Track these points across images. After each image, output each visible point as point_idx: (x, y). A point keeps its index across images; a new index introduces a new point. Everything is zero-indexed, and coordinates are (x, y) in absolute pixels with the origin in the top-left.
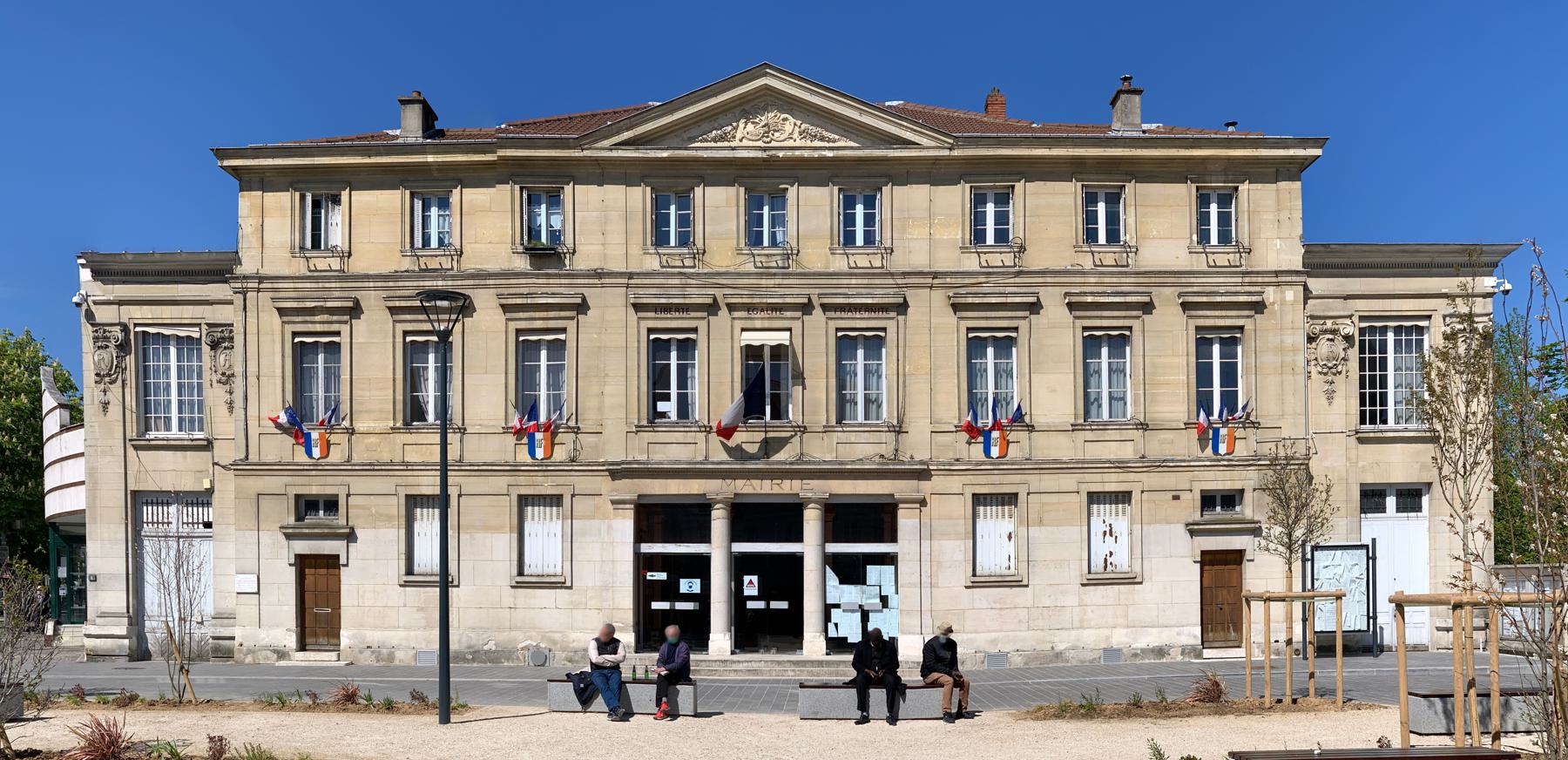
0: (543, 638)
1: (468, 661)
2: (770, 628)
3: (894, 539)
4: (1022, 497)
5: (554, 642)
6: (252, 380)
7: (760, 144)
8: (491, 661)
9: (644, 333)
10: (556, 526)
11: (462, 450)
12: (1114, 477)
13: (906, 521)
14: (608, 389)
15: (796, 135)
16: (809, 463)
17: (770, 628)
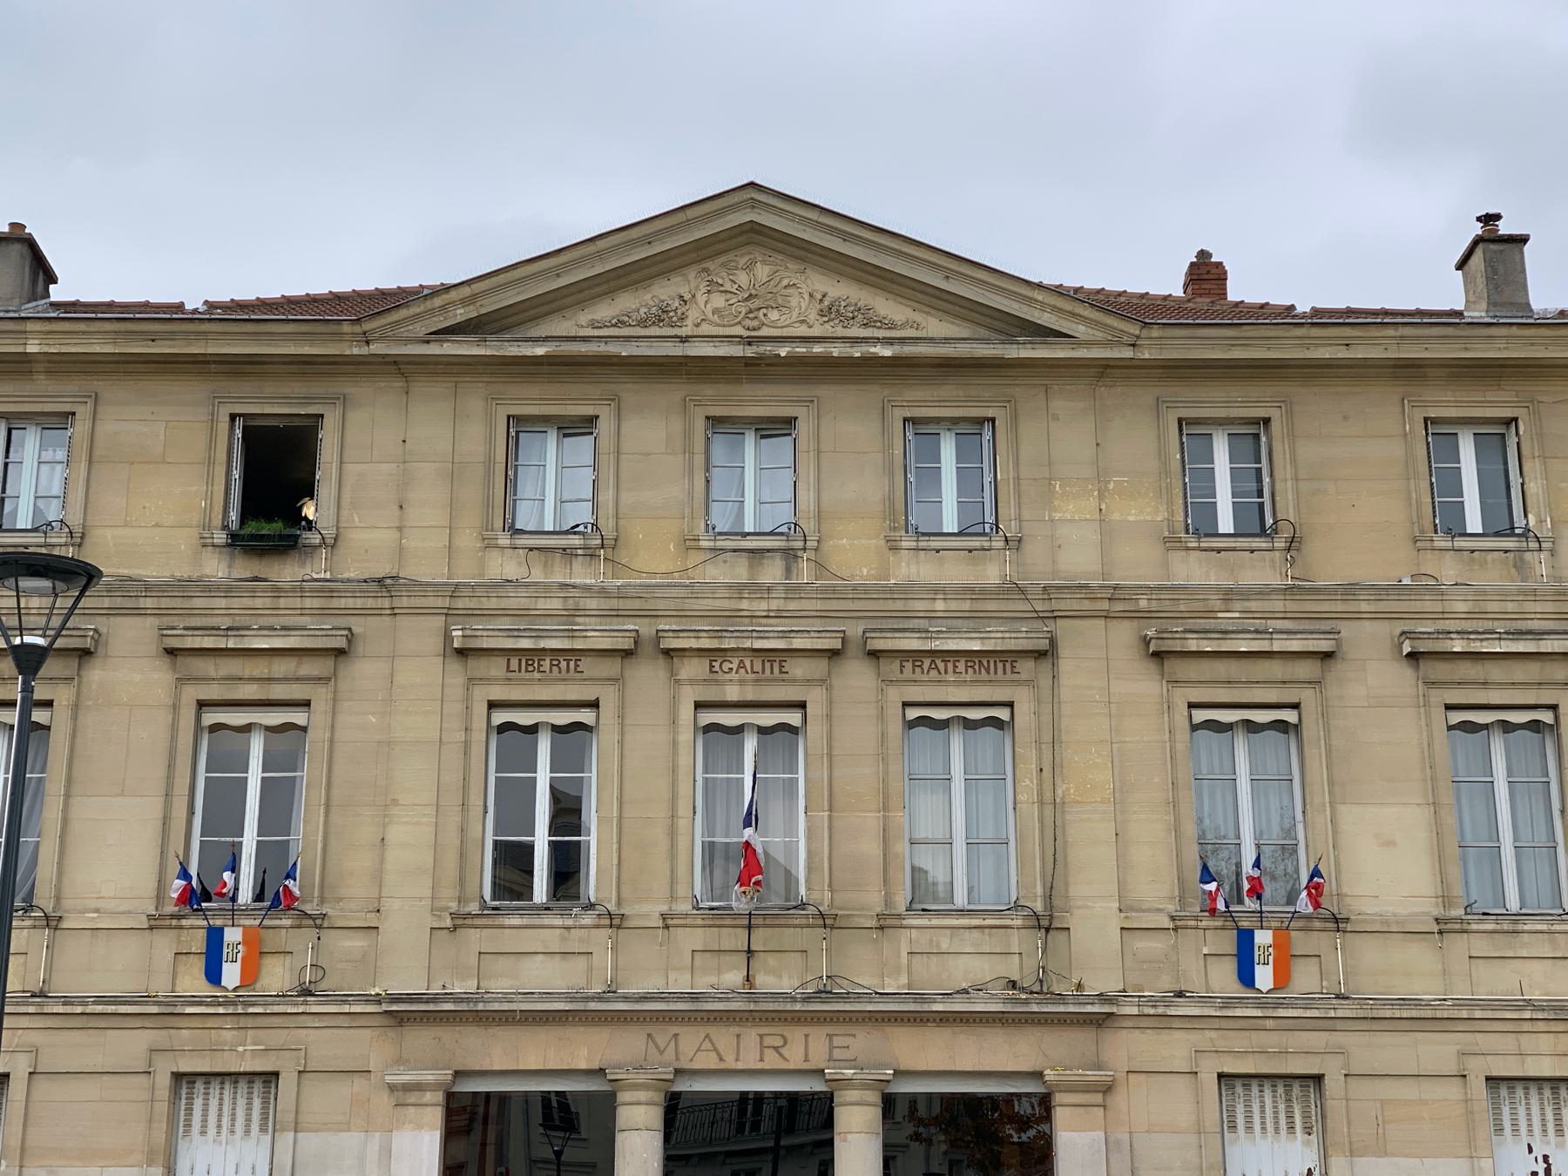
4: (1333, 1084)
7: (739, 331)
11: (49, 969)
12: (1545, 1043)
14: (395, 834)
15: (813, 316)
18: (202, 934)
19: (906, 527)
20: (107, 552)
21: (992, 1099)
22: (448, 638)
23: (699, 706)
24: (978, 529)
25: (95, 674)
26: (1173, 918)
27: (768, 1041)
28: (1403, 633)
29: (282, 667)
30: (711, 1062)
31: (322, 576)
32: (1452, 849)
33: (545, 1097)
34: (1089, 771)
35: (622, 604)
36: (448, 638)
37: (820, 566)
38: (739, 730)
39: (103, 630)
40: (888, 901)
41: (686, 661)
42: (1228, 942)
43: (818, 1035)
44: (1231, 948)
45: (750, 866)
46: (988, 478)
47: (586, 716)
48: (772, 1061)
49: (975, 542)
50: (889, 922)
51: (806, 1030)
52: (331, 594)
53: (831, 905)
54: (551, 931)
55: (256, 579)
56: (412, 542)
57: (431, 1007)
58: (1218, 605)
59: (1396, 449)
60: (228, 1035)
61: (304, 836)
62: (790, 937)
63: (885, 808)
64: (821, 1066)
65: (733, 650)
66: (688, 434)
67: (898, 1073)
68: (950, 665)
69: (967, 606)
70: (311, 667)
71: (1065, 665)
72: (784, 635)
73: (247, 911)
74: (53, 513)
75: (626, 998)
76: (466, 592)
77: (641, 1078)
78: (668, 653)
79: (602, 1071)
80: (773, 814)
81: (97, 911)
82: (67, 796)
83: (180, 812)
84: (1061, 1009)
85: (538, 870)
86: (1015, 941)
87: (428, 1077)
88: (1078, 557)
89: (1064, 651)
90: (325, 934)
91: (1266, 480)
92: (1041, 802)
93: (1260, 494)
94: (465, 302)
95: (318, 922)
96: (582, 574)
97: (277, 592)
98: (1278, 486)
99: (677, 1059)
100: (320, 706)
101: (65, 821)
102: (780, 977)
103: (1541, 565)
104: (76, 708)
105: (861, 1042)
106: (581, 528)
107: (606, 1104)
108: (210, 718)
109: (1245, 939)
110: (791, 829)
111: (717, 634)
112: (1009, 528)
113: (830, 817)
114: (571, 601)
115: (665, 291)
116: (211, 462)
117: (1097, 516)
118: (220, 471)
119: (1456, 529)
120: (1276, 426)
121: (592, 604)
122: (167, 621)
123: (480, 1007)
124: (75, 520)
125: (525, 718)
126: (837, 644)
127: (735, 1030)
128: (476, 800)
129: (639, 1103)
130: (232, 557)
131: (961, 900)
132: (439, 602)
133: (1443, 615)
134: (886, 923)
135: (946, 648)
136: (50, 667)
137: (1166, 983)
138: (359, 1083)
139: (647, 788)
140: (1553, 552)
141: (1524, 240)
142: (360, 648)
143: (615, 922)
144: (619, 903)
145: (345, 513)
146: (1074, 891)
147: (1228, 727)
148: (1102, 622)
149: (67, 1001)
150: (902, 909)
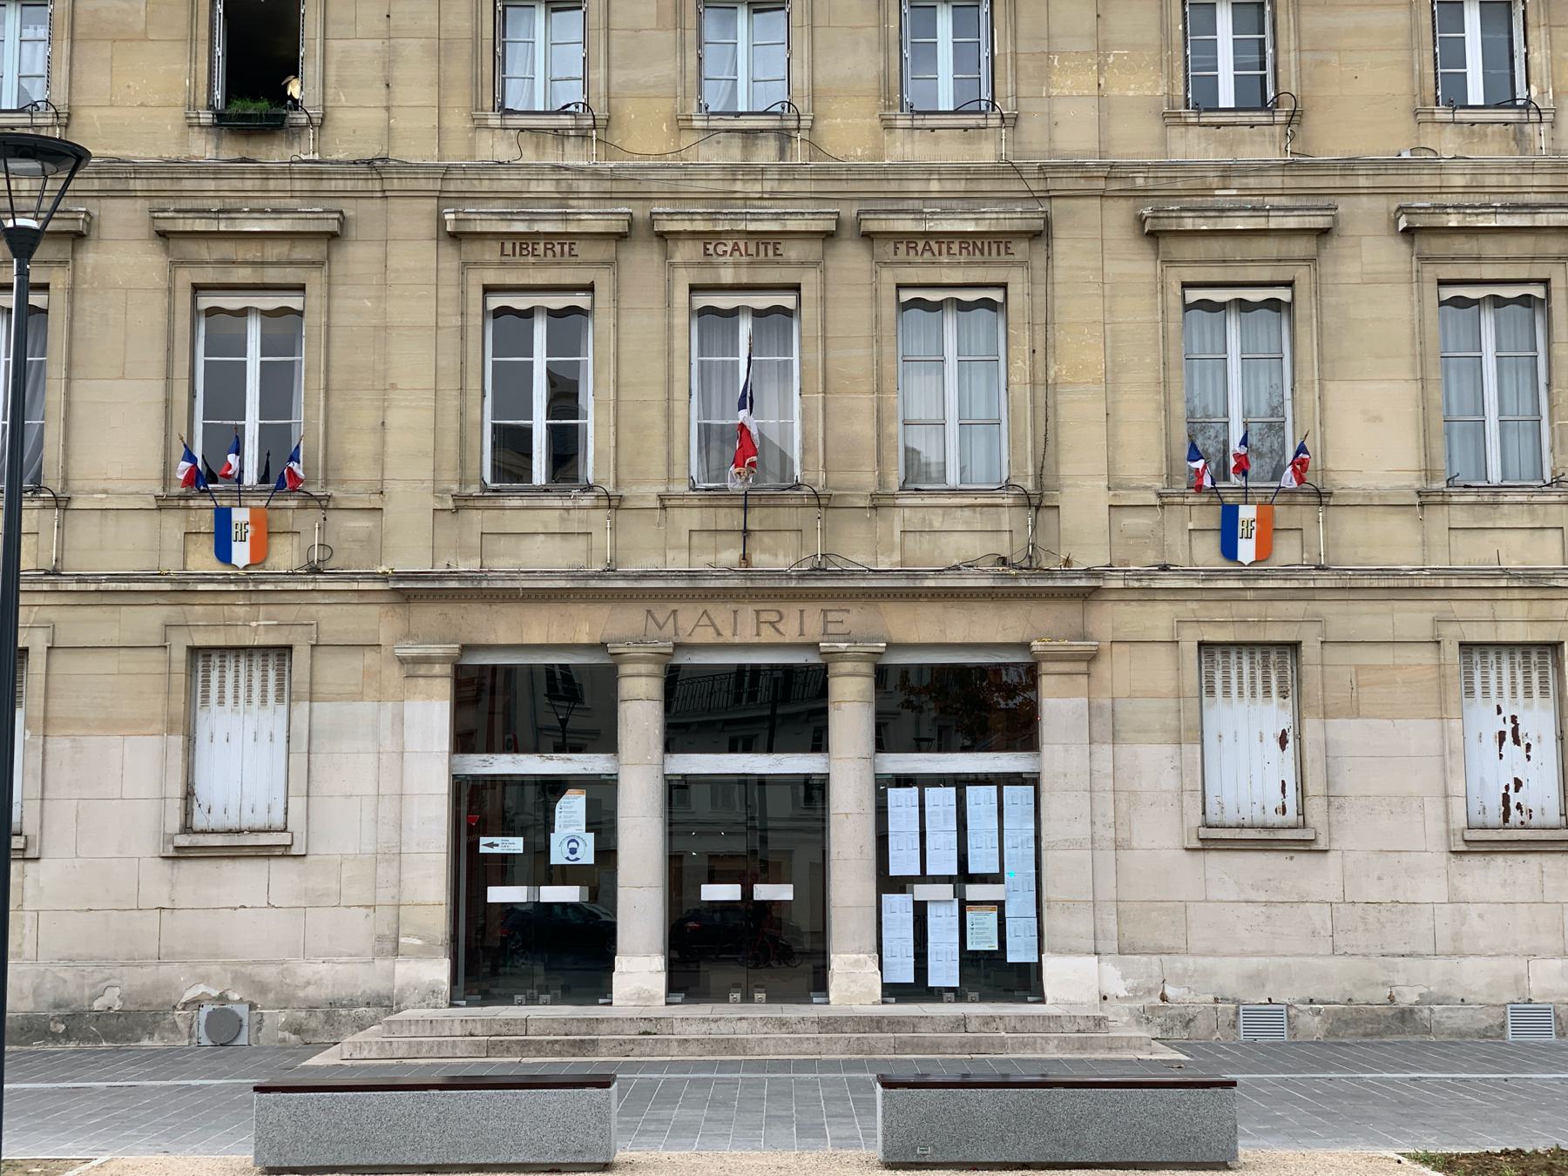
0: (237, 978)
1: (55, 1037)
2: (745, 944)
4: (1309, 651)
5: (262, 988)
8: (109, 1037)
9: (476, 294)
11: (61, 547)
12: (1519, 610)
13: (1059, 706)
14: (395, 418)
16: (840, 574)
17: (745, 944)
18: (210, 514)
19: (900, 105)
20: (97, 132)
21: (982, 670)
22: (441, 221)
23: (694, 289)
24: (974, 106)
25: (90, 257)
26: (1160, 495)
27: (764, 617)
28: (1400, 208)
29: (274, 251)
31: (311, 157)
32: (1437, 423)
33: (550, 669)
34: (1080, 352)
35: (615, 186)
36: (441, 221)
38: (734, 312)
39: (95, 212)
40: (882, 482)
41: (680, 244)
42: (1212, 518)
43: (813, 612)
45: (745, 447)
46: (985, 53)
47: (582, 300)
48: (768, 635)
49: (970, 121)
50: (882, 502)
51: (801, 606)
52: (319, 175)
53: (826, 486)
54: (550, 513)
56: (400, 122)
57: (437, 585)
58: (1216, 182)
59: (1400, 18)
60: (241, 611)
61: (306, 418)
62: (785, 517)
64: (816, 640)
65: (727, 232)
67: (890, 646)
68: (944, 247)
69: (961, 186)
70: (303, 251)
71: (1060, 246)
73: (252, 493)
74: (37, 93)
75: (625, 577)
76: (457, 174)
78: (663, 236)
80: (768, 397)
81: (105, 492)
82: (69, 379)
83: (181, 395)
84: (1050, 583)
85: (535, 452)
86: (1006, 519)
87: (437, 650)
89: (1059, 232)
90: (333, 517)
91: (1269, 51)
92: (1033, 384)
93: (1263, 67)
95: (324, 503)
96: (574, 156)
97: (266, 174)
98: (1282, 58)
99: (676, 634)
101: (68, 404)
102: (776, 555)
103: (1540, 138)
104: (72, 291)
105: (854, 618)
106: (572, 108)
107: (607, 678)
108: (206, 302)
109: (1230, 514)
110: (785, 411)
111: (711, 217)
112: (1006, 105)
113: (824, 398)
114: (563, 184)
116: (193, 39)
117: (1096, 92)
118: (203, 49)
119: (1457, 100)
121: (585, 186)
122: (157, 203)
123: (484, 584)
124: (60, 99)
125: (520, 302)
126: (831, 226)
127: (732, 606)
128: (473, 384)
129: (640, 676)
130: (219, 138)
131: (953, 479)
132: (431, 185)
133: (1441, 190)
134: (879, 503)
135: (939, 229)
136: (44, 251)
137: (1152, 557)
138: (370, 657)
139: (643, 374)
140: (1553, 124)
142: (352, 232)
143: (614, 503)
144: (617, 485)
145: (330, 91)
146: (1063, 471)
148: (1097, 202)
149: (81, 579)
150: (895, 489)
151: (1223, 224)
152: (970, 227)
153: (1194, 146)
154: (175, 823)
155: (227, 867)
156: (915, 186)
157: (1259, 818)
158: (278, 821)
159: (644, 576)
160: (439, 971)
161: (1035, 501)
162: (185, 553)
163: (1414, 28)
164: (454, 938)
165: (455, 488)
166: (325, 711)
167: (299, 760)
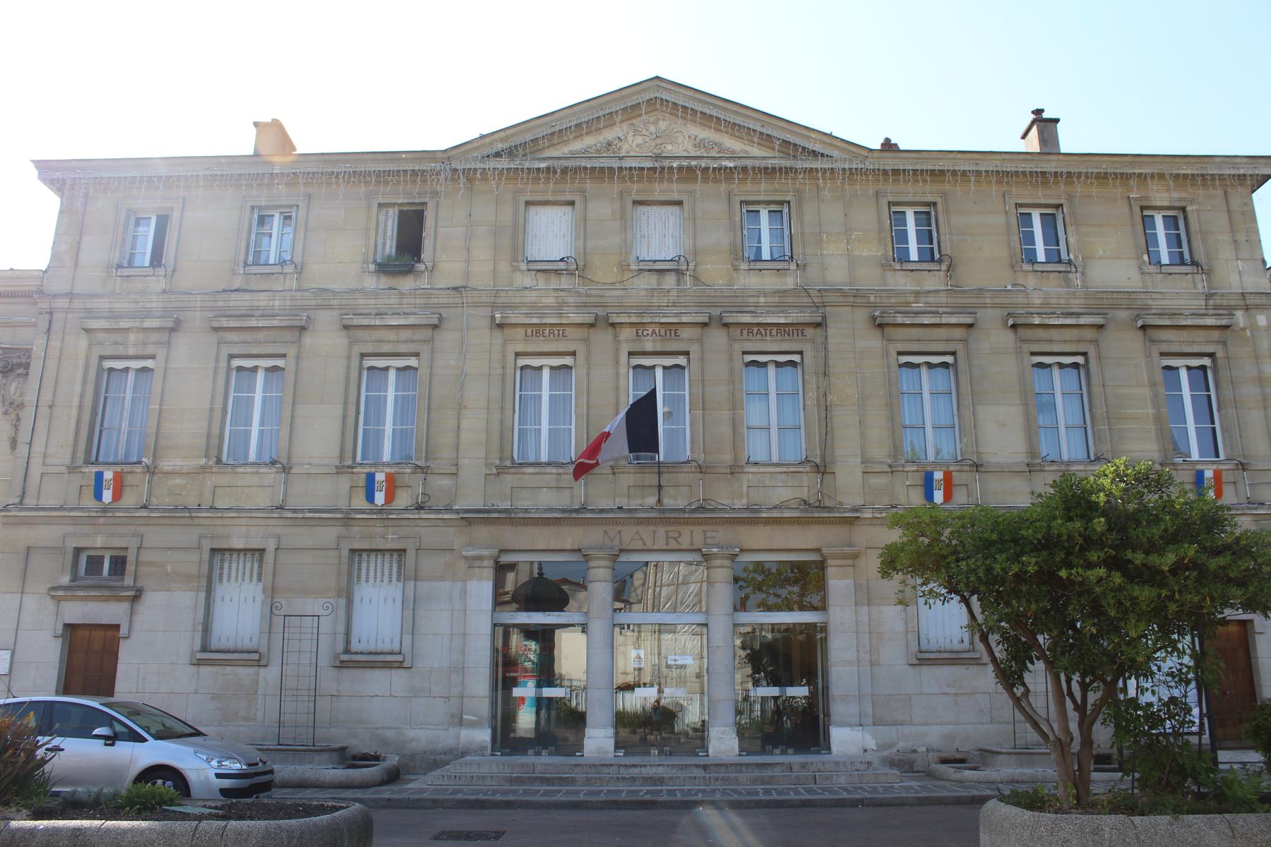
3: (822, 607)
6: (43, 410)
9: (511, 357)
10: (393, 591)
11: (285, 494)
14: (465, 424)
15: (690, 147)
18: (364, 476)
23: (630, 354)
25: (308, 340)
26: (890, 466)
30: (640, 546)
35: (588, 300)
36: (493, 317)
37: (696, 278)
42: (918, 479)
43: (698, 530)
44: (920, 482)
46: (787, 233)
48: (673, 545)
55: (391, 288)
59: (1001, 220)
60: (379, 530)
63: (734, 408)
66: (623, 210)
69: (777, 299)
72: (677, 315)
75: (592, 511)
77: (601, 554)
78: (613, 325)
79: (579, 550)
82: (294, 404)
83: (352, 412)
87: (485, 552)
88: (837, 274)
89: (830, 324)
90: (430, 478)
91: (935, 234)
92: (819, 405)
93: (931, 243)
94: (502, 140)
96: (565, 282)
97: (402, 295)
98: (942, 238)
100: (425, 355)
101: (293, 417)
103: (1076, 279)
115: (609, 135)
118: (373, 233)
119: (1032, 260)
120: (940, 207)
124: (297, 259)
125: (535, 362)
127: (652, 528)
137: (887, 501)
140: (1083, 274)
141: (1057, 121)
145: (438, 254)
146: (838, 452)
147: (918, 366)
148: (849, 309)
149: (294, 511)
151: (918, 320)
152: (782, 321)
153: (901, 282)
154: (340, 648)
155: (369, 674)
156: (752, 300)
157: (949, 647)
158: (396, 647)
159: (602, 511)
160: (483, 736)
161: (822, 469)
162: (350, 497)
163: (1008, 225)
164: (494, 717)
165: (497, 462)
166: (423, 586)
167: (409, 613)
